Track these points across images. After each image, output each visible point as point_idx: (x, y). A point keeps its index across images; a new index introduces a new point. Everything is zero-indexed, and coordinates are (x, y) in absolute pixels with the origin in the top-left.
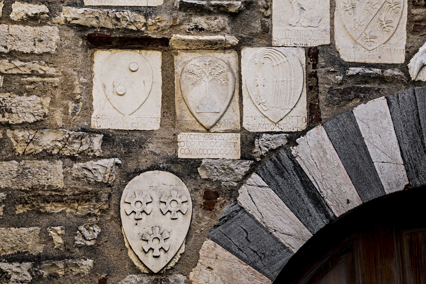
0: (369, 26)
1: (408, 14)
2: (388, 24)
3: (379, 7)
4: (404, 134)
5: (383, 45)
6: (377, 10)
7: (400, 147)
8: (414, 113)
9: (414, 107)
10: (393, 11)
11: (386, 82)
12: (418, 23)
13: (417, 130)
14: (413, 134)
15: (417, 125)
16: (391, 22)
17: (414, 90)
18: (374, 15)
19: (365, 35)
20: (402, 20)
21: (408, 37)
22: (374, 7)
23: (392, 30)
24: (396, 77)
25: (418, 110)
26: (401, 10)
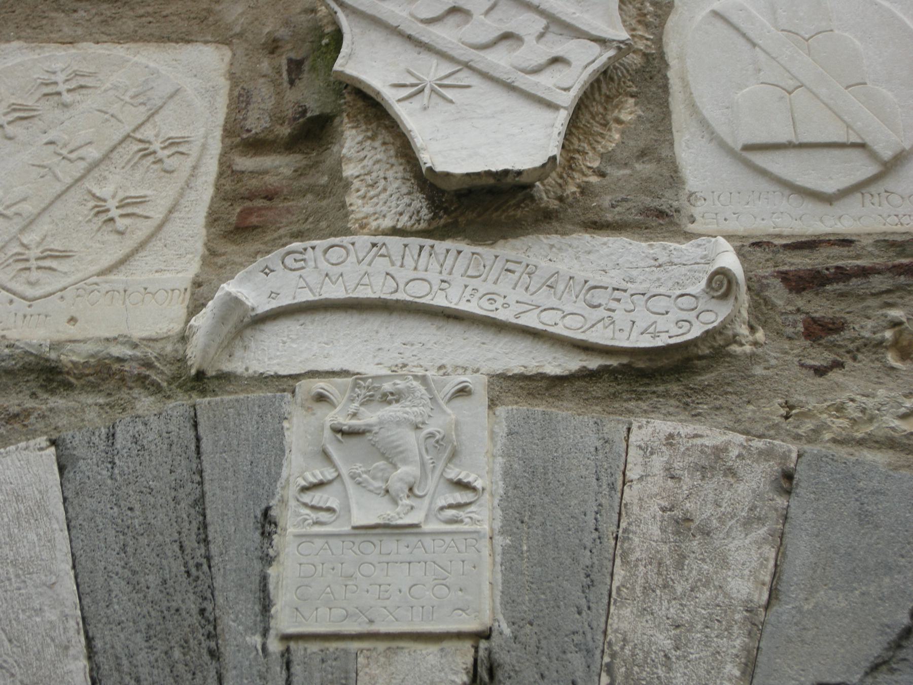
0: (46, 218)
1: (221, 174)
2: (129, 210)
3: (93, 153)
4: (118, 585)
5: (95, 279)
6: (82, 165)
7: (89, 640)
8: (181, 493)
9: (183, 472)
10: (155, 167)
11: (69, 386)
12: (259, 203)
13: (186, 564)
14: (165, 582)
15: (190, 542)
16: (141, 201)
17: (194, 406)
18: (69, 180)
19: (19, 249)
20: (192, 195)
21: (212, 253)
22: (73, 156)
23: (143, 229)
24: (116, 366)
25: (201, 483)
26: (189, 162)
